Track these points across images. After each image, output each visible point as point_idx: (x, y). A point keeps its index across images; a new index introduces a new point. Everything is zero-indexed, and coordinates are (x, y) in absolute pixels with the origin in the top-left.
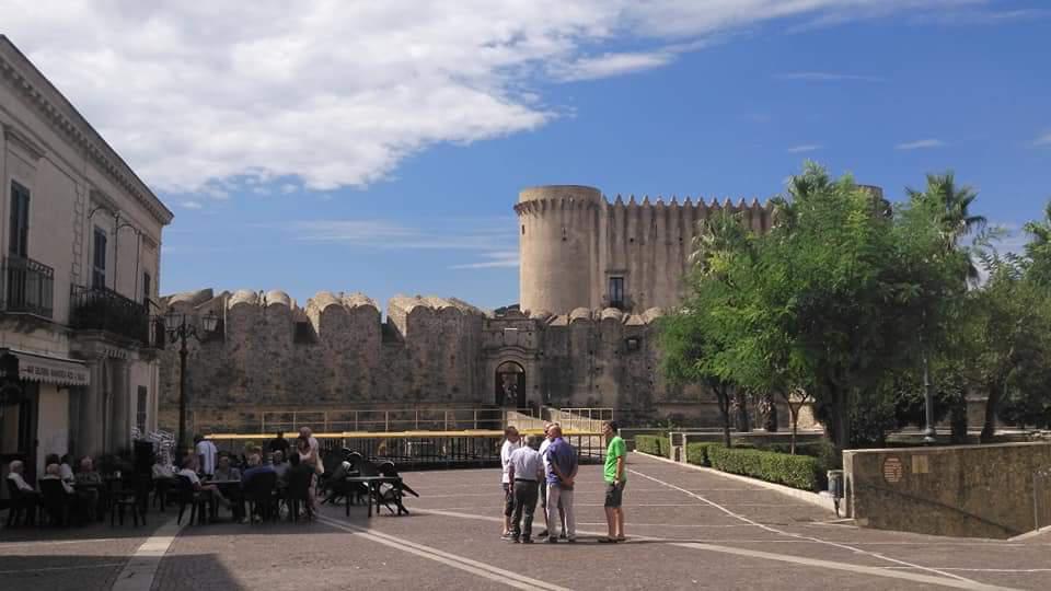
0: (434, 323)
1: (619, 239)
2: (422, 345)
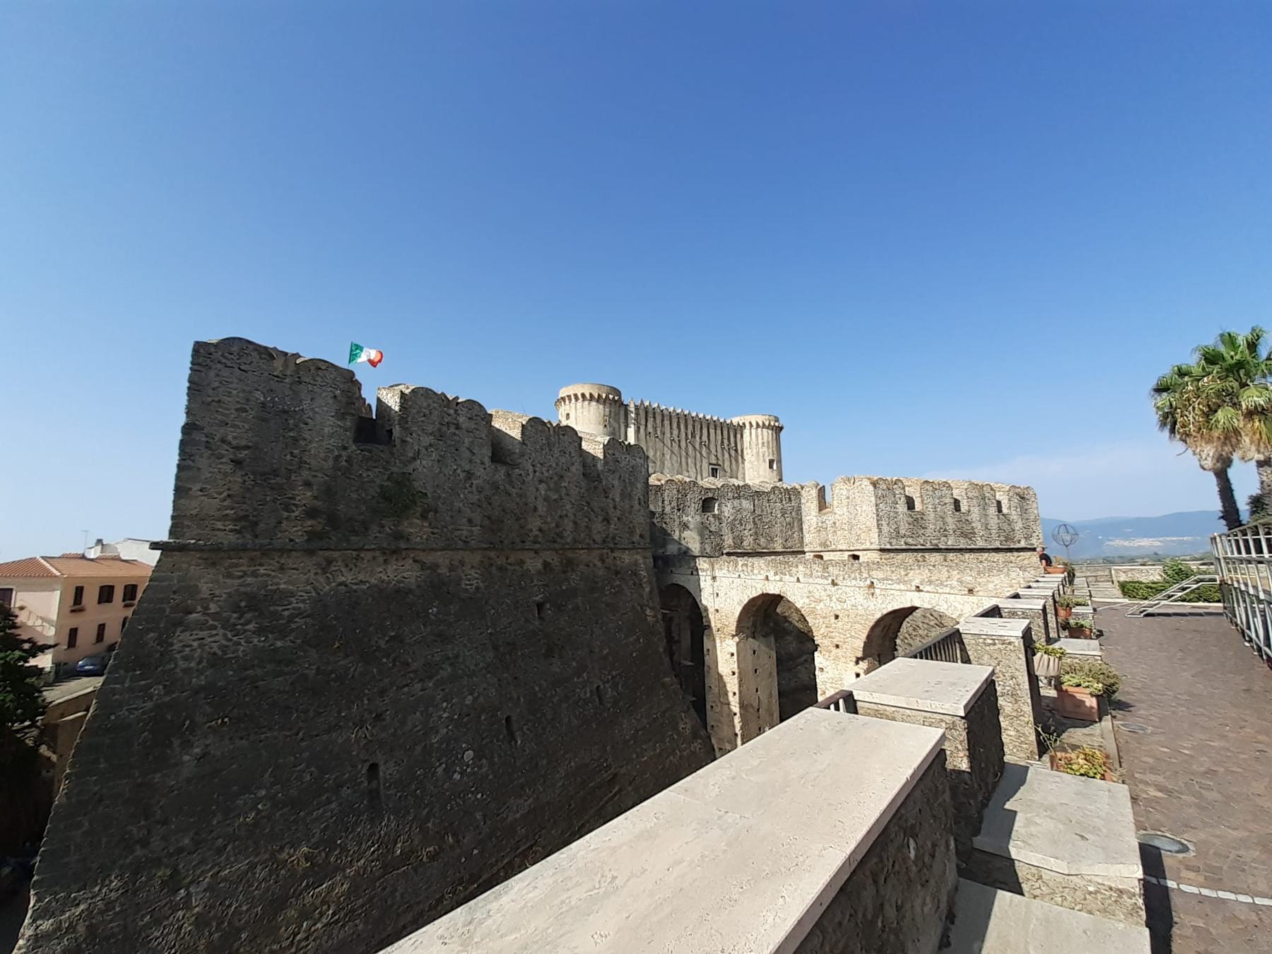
0: (625, 460)
2: (616, 483)
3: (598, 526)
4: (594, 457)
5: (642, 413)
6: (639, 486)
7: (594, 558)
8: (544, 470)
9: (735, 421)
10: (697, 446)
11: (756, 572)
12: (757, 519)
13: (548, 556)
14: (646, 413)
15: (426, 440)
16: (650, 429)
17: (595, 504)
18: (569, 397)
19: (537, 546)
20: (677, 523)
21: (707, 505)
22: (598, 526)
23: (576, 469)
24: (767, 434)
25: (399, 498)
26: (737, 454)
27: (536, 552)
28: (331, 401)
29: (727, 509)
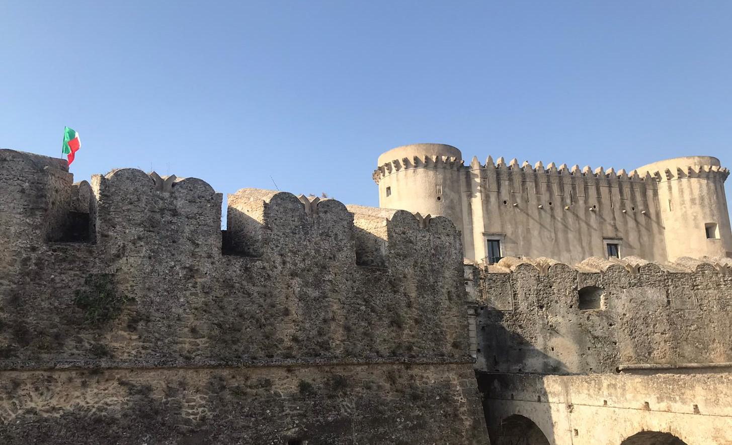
0: (423, 239)
1: (493, 199)
2: (409, 271)
3: (382, 332)
4: (376, 240)
5: (492, 176)
6: (447, 274)
7: (378, 375)
8: (298, 259)
9: (642, 172)
10: (581, 214)
11: (629, 396)
12: (675, 319)
13: (308, 375)
14: (498, 175)
15: (134, 232)
16: (505, 196)
17: (377, 302)
18: (387, 165)
19: (289, 362)
20: (539, 326)
21: (586, 297)
22: (382, 332)
23: (347, 255)
24: (697, 186)
25: (99, 305)
26: (649, 221)
27: (289, 369)
28: (18, 196)
29: (618, 303)
